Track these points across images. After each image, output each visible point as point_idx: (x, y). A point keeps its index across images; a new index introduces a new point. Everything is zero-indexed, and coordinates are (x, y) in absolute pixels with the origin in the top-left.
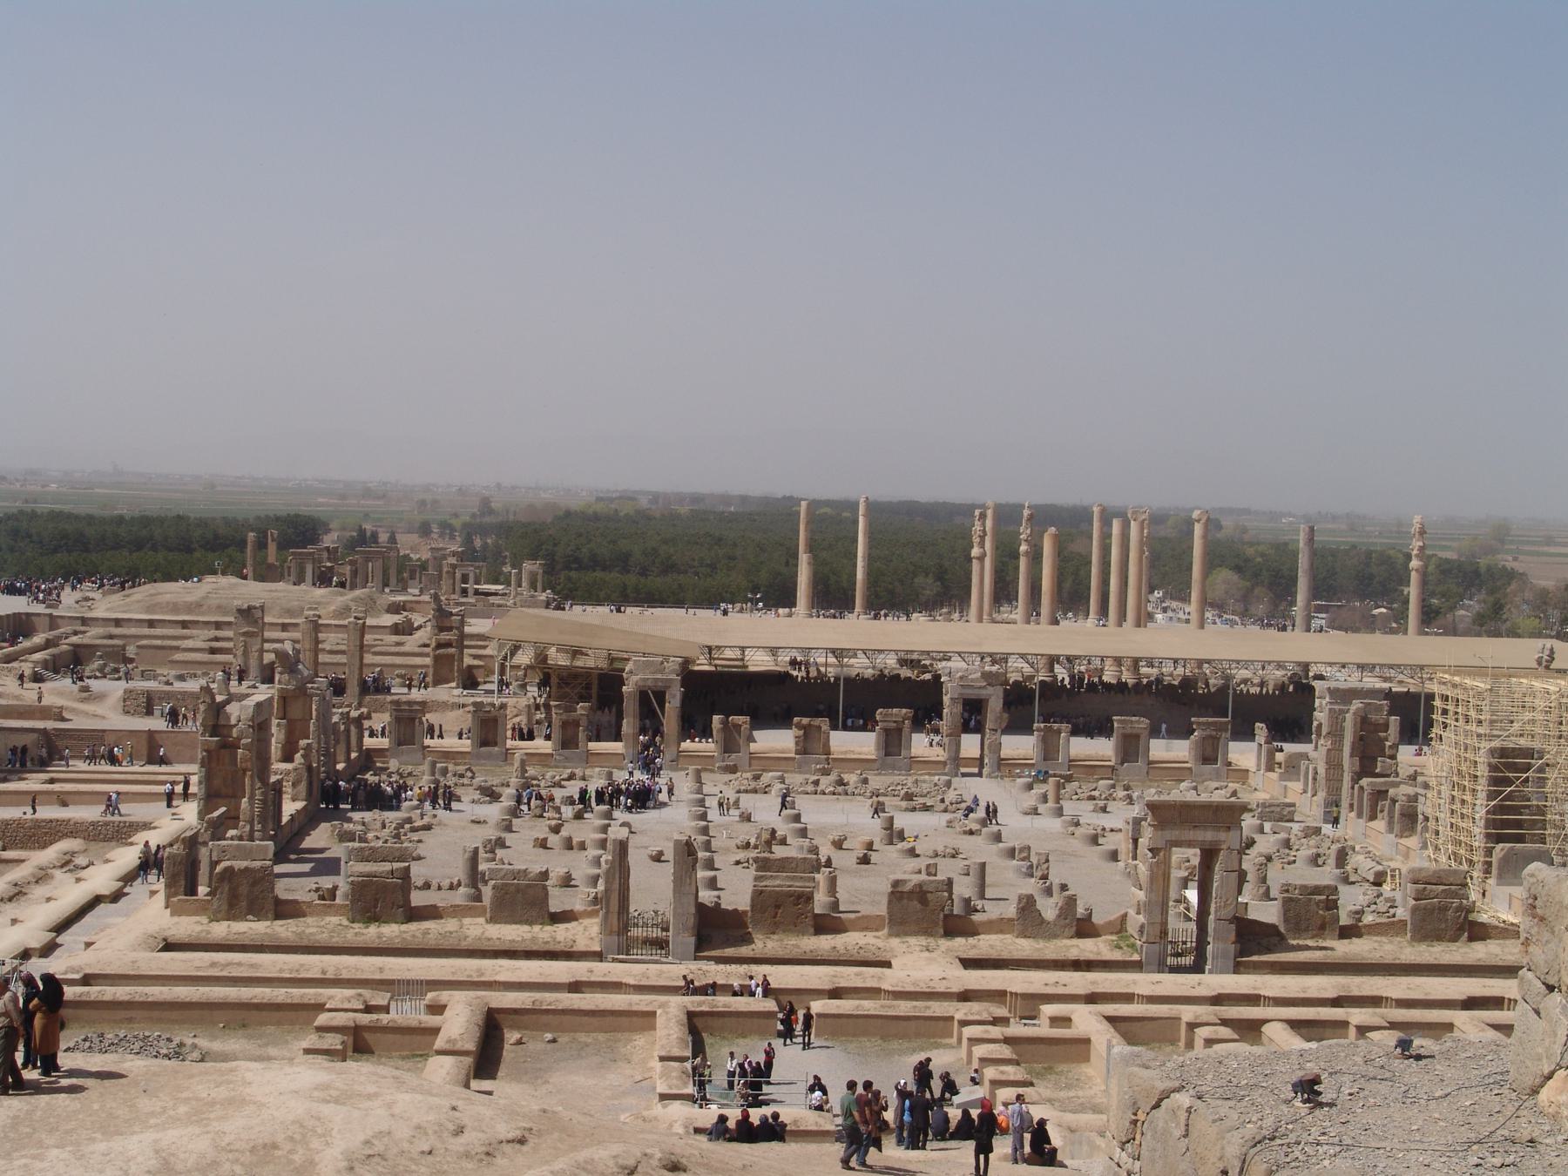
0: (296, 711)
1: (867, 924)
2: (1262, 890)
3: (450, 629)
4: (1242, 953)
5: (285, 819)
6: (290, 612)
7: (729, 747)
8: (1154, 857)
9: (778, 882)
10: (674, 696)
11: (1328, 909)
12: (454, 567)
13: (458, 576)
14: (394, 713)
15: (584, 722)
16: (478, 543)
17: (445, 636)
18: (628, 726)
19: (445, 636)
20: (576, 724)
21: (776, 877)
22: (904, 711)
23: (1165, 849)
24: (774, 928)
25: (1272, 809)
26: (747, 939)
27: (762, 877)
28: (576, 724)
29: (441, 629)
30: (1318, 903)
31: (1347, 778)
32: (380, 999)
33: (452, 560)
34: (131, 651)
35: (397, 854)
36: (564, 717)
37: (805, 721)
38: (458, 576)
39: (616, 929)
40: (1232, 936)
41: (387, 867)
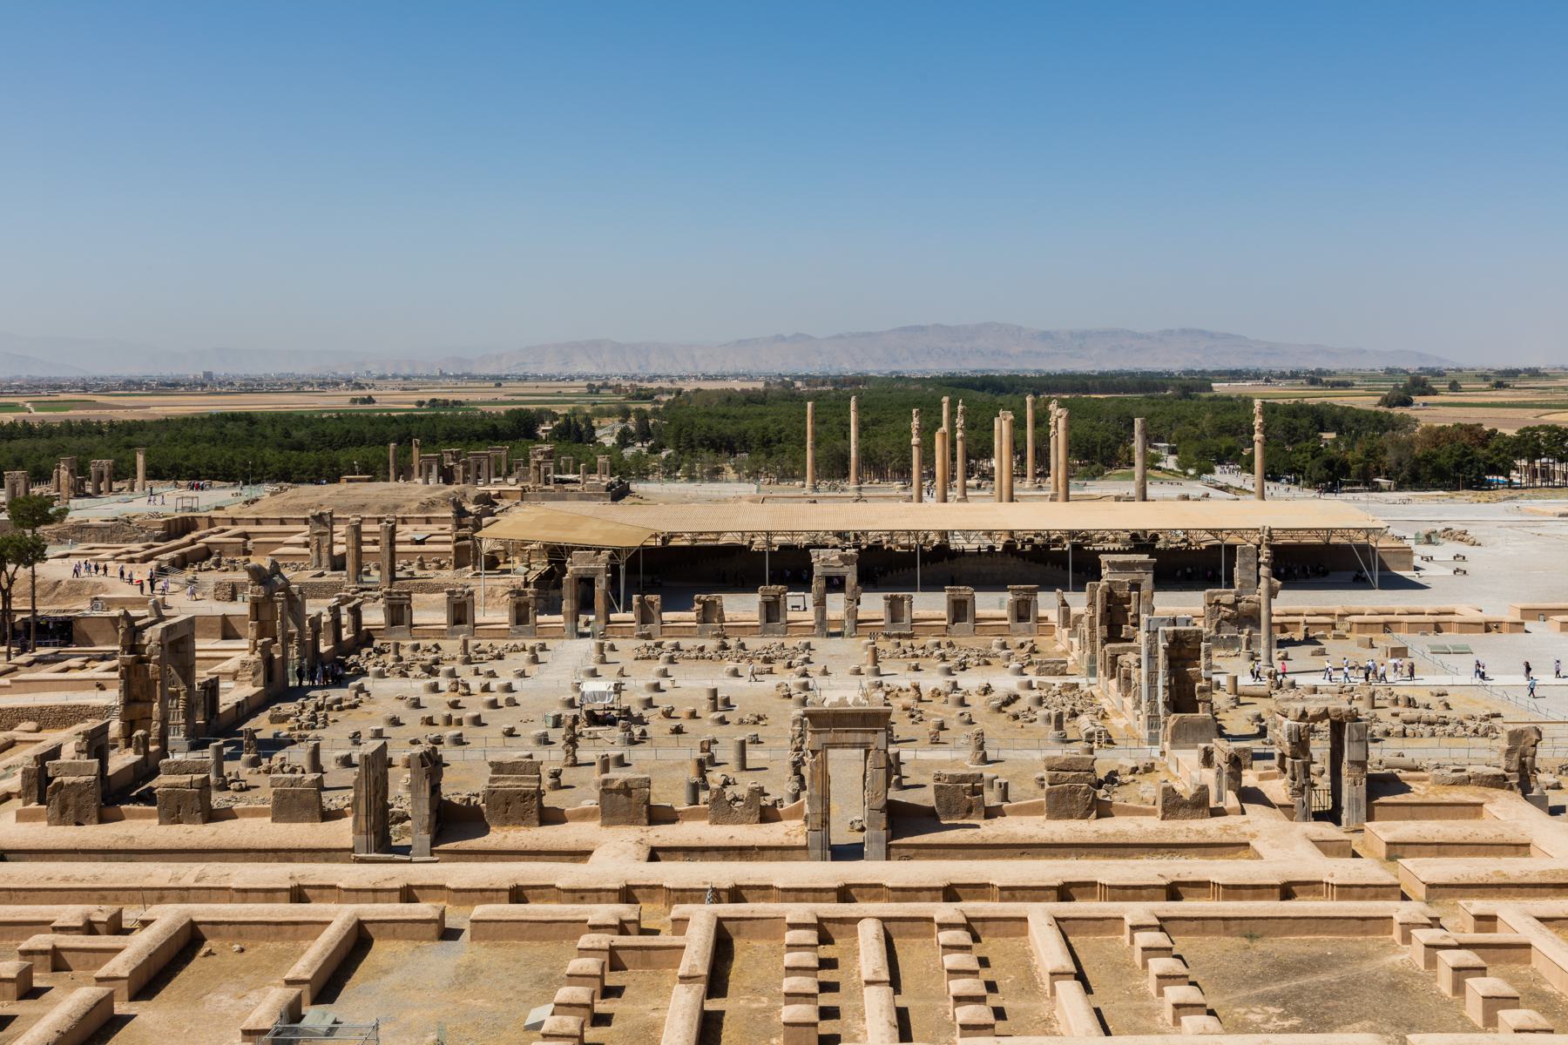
0: (265, 615)
1: (584, 815)
2: (979, 756)
3: (466, 526)
4: (892, 839)
5: (222, 709)
6: (384, 509)
7: (645, 618)
8: (814, 757)
9: (508, 783)
10: (601, 581)
11: (974, 794)
12: (539, 463)
13: (542, 470)
14: (388, 601)
15: (532, 603)
17: (462, 532)
18: (567, 605)
19: (462, 532)
20: (527, 605)
21: (507, 779)
22: (780, 587)
23: (822, 750)
24: (506, 821)
25: (1047, 666)
26: (485, 830)
27: (495, 779)
28: (527, 605)
29: (460, 526)
30: (964, 791)
31: (1098, 642)
32: (101, 913)
33: (540, 458)
34: (250, 545)
35: (198, 767)
36: (517, 600)
37: (703, 597)
38: (542, 470)
39: (364, 829)
40: (884, 826)
41: (187, 778)
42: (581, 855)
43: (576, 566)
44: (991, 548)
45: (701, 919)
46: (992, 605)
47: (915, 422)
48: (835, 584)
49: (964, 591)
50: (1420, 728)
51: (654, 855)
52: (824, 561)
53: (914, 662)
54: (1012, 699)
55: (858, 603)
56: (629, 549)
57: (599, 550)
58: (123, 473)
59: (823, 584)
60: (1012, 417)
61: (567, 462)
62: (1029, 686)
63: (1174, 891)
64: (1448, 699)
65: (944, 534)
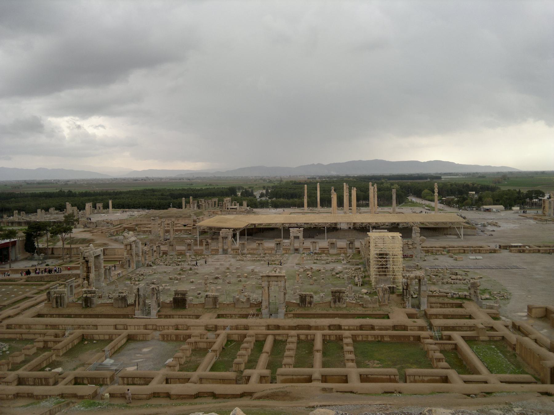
16: (269, 191)
38: (226, 205)
42: (198, 317)
43: (222, 233)
44: (350, 228)
45: (223, 334)
46: (342, 243)
47: (333, 191)
48: (297, 238)
49: (334, 240)
51: (219, 316)
52: (293, 232)
53: (315, 261)
54: (341, 272)
55: (303, 243)
56: (239, 229)
57: (229, 229)
58: (106, 207)
59: (292, 238)
60: (356, 189)
61: (235, 203)
62: (346, 268)
63: (361, 328)
65: (336, 224)
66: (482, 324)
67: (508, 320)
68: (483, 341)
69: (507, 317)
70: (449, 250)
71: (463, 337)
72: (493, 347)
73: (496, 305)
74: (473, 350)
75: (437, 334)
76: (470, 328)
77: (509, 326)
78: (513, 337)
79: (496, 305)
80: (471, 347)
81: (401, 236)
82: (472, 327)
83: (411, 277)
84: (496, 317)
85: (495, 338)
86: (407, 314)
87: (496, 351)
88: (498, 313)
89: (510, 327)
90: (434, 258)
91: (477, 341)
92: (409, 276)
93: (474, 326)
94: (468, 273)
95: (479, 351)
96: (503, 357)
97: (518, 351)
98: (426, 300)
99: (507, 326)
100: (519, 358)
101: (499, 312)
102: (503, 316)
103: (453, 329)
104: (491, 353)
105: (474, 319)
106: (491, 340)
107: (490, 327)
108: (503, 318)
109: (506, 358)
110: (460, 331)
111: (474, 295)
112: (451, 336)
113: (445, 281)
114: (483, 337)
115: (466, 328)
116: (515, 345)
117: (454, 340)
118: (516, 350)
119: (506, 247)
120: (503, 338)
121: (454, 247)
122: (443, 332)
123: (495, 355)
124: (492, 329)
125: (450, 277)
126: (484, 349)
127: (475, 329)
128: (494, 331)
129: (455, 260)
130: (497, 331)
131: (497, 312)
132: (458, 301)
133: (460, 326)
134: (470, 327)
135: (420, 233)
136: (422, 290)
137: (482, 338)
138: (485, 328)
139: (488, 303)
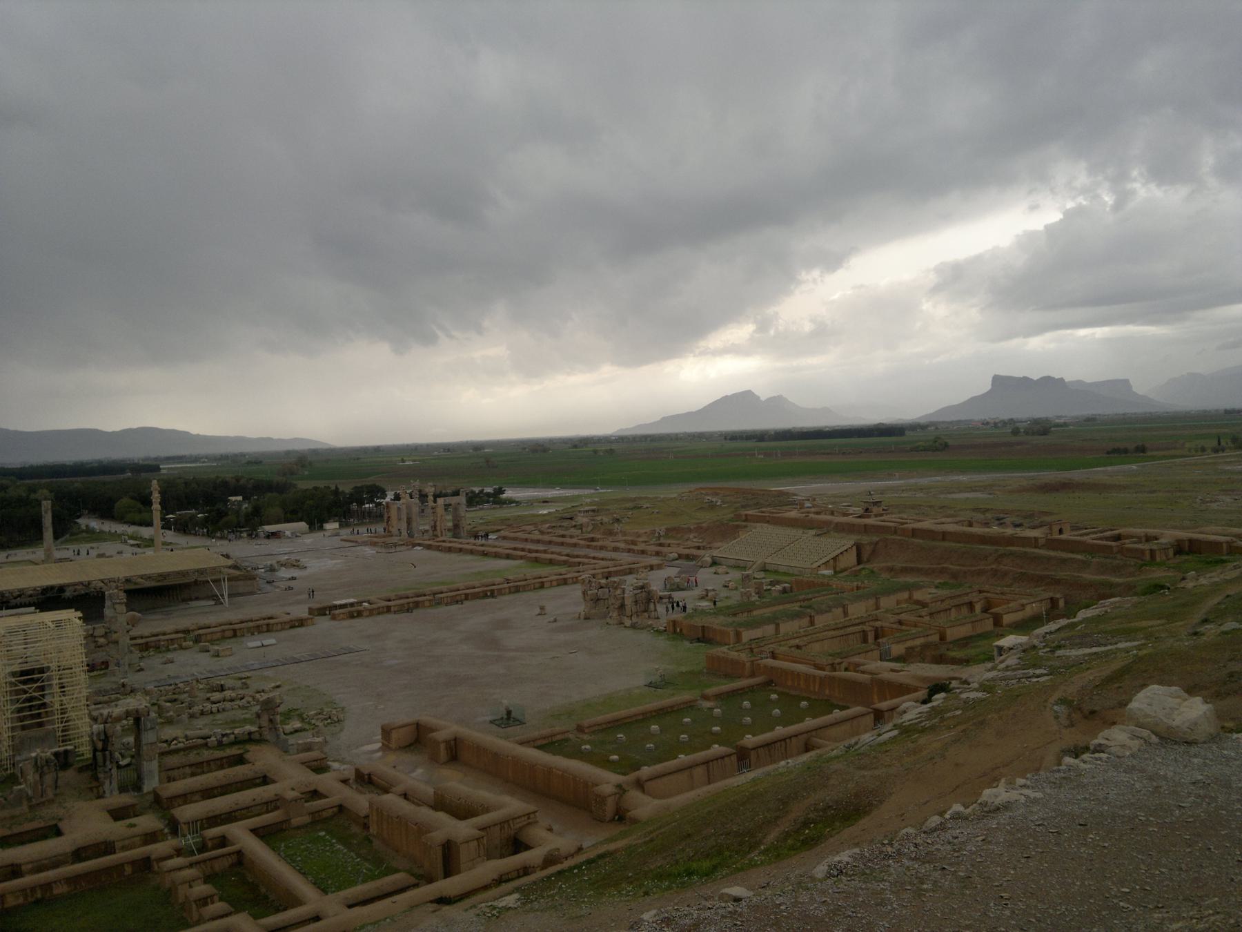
50: (228, 705)
64: (248, 682)
66: (293, 789)
67: (345, 766)
68: (298, 828)
69: (342, 762)
70: (199, 635)
71: (255, 831)
72: (322, 834)
73: (317, 740)
74: (279, 854)
75: (190, 841)
76: (267, 806)
77: (349, 779)
78: (361, 801)
79: (317, 740)
80: (273, 849)
81: (80, 618)
82: (271, 802)
83: (114, 715)
84: (320, 768)
85: (325, 814)
86: (108, 811)
87: (329, 841)
88: (324, 756)
89: (351, 781)
90: (165, 659)
91: (285, 830)
92: (109, 716)
93: (277, 798)
94: (248, 682)
95: (292, 852)
96: (345, 851)
97: (373, 830)
98: (157, 764)
99: (345, 781)
100: (376, 843)
101: (325, 754)
102: (334, 761)
103: (229, 817)
104: (318, 850)
105: (274, 782)
106: (318, 820)
107: (310, 792)
108: (335, 765)
109: (353, 851)
110: (244, 819)
111: (270, 729)
112: (227, 835)
113: (196, 709)
114: (299, 819)
115: (259, 807)
116: (367, 817)
117: (233, 844)
118: (369, 827)
119: (322, 612)
120: (341, 808)
121: (209, 627)
122: (207, 831)
123: (328, 851)
124: (315, 794)
125: (208, 699)
126: (302, 844)
127: (278, 804)
128: (320, 799)
129: (214, 656)
130: (327, 797)
131: (322, 755)
132: (235, 751)
133: (245, 806)
134: (267, 803)
135: (127, 605)
136: (144, 742)
137: (296, 821)
138: (303, 796)
139: (306, 738)
